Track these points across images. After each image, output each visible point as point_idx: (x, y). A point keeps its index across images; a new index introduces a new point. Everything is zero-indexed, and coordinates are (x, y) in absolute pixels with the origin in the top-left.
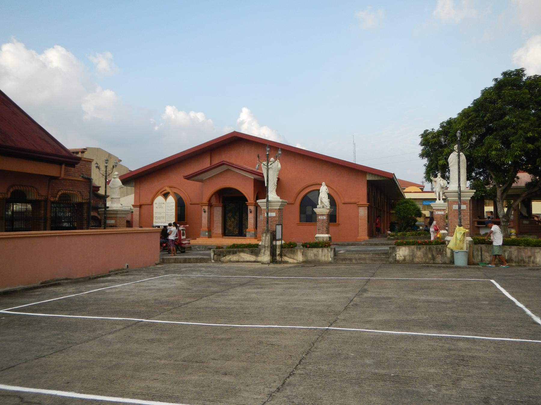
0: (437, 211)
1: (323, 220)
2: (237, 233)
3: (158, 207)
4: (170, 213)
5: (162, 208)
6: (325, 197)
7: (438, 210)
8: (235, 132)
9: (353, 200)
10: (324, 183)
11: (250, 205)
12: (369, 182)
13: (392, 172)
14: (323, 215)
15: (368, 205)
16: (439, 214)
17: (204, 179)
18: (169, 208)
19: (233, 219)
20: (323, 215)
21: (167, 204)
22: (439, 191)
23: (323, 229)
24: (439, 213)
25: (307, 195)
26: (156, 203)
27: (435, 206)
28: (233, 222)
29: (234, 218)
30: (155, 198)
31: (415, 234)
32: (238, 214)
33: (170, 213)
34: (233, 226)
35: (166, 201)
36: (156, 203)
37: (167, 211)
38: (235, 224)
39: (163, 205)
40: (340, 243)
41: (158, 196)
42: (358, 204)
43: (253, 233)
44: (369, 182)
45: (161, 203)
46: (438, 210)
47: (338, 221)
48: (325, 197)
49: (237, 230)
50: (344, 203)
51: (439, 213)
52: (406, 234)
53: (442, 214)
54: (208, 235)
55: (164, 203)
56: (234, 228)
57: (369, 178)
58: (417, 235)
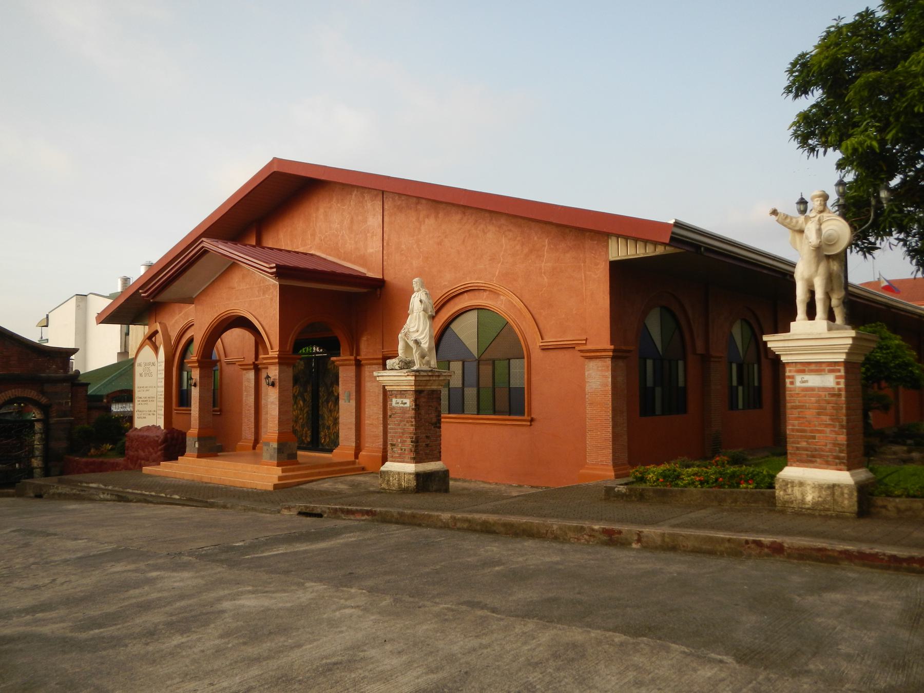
0: (803, 371)
1: (404, 411)
2: (309, 440)
6: (420, 330)
7: (806, 367)
8: (275, 159)
9: (568, 338)
10: (416, 280)
11: (342, 365)
12: (619, 270)
13: (270, 159)
14: (402, 394)
15: (611, 354)
16: (812, 389)
17: (194, 297)
19: (301, 402)
20: (402, 394)
22: (806, 275)
23: (403, 442)
24: (814, 381)
25: (453, 326)
26: (140, 365)
27: (790, 351)
28: (301, 410)
31: (717, 480)
36: (140, 365)
38: (305, 415)
39: (153, 369)
40: (378, 509)
42: (581, 351)
43: (274, 448)
44: (619, 270)
45: (149, 364)
46: (806, 367)
47: (530, 413)
48: (420, 330)
49: (309, 433)
50: (544, 349)
51: (814, 381)
52: (678, 477)
53: (824, 389)
54: (199, 449)
55: (154, 364)
56: (303, 426)
57: (619, 251)
58: (721, 486)
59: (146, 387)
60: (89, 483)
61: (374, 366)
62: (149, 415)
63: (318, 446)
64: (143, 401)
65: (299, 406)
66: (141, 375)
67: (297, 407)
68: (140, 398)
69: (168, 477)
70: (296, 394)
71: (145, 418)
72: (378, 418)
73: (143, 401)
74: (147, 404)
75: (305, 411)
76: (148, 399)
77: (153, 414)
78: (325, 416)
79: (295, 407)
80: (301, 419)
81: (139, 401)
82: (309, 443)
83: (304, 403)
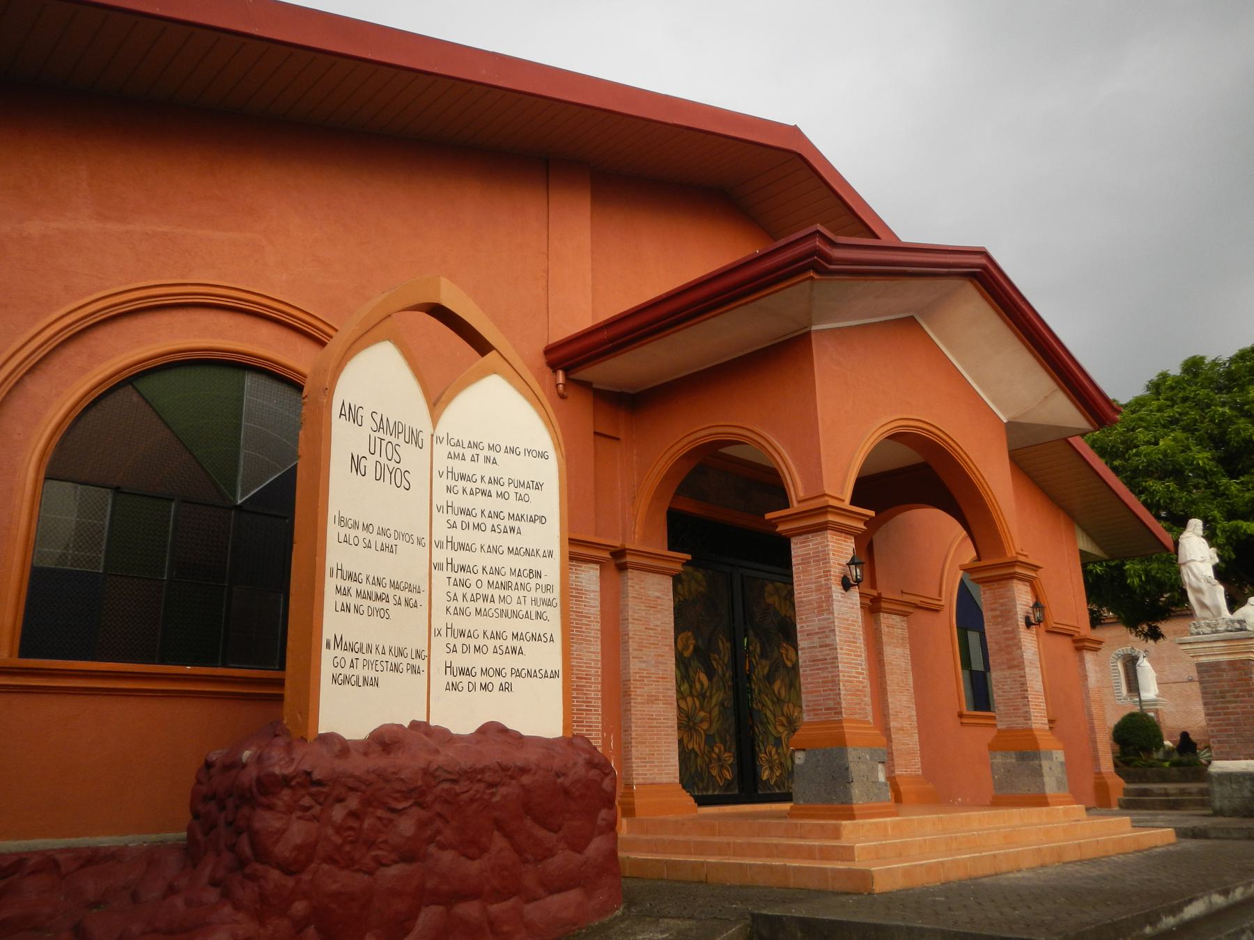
3: (369, 464)
4: (492, 560)
5: (400, 479)
18: (478, 502)
21: (441, 450)
28: (702, 696)
29: (710, 674)
30: (354, 355)
32: (724, 646)
33: (492, 560)
34: (705, 726)
35: (435, 419)
37: (441, 533)
38: (716, 712)
39: (411, 457)
41: (376, 341)
43: (1061, 763)
45: (396, 429)
49: (729, 758)
55: (414, 438)
59: (383, 532)
60: (1179, 909)
61: (894, 616)
62: (395, 668)
63: (756, 791)
64: (368, 596)
65: (698, 686)
66: (356, 464)
67: (691, 687)
68: (352, 577)
69: (1002, 873)
70: (686, 654)
71: (375, 682)
72: (910, 717)
73: (368, 596)
74: (383, 614)
75: (714, 701)
76: (389, 591)
77: (415, 670)
78: (769, 714)
79: (685, 687)
80: (702, 721)
81: (346, 592)
82: (729, 785)
83: (710, 679)
